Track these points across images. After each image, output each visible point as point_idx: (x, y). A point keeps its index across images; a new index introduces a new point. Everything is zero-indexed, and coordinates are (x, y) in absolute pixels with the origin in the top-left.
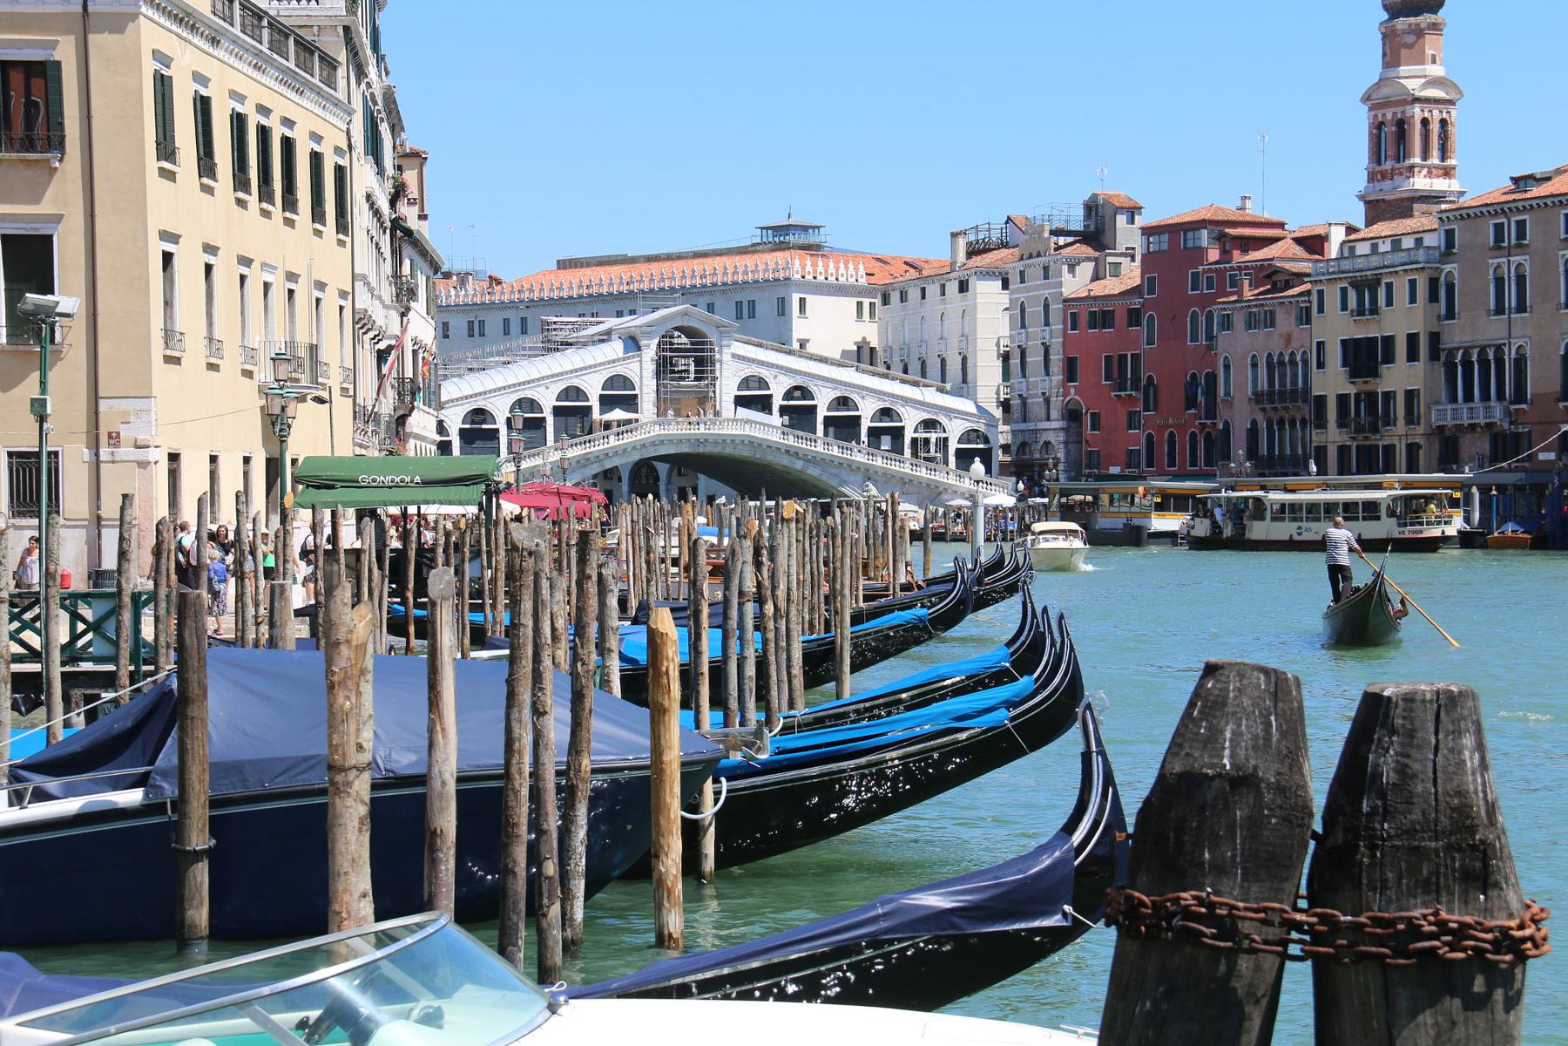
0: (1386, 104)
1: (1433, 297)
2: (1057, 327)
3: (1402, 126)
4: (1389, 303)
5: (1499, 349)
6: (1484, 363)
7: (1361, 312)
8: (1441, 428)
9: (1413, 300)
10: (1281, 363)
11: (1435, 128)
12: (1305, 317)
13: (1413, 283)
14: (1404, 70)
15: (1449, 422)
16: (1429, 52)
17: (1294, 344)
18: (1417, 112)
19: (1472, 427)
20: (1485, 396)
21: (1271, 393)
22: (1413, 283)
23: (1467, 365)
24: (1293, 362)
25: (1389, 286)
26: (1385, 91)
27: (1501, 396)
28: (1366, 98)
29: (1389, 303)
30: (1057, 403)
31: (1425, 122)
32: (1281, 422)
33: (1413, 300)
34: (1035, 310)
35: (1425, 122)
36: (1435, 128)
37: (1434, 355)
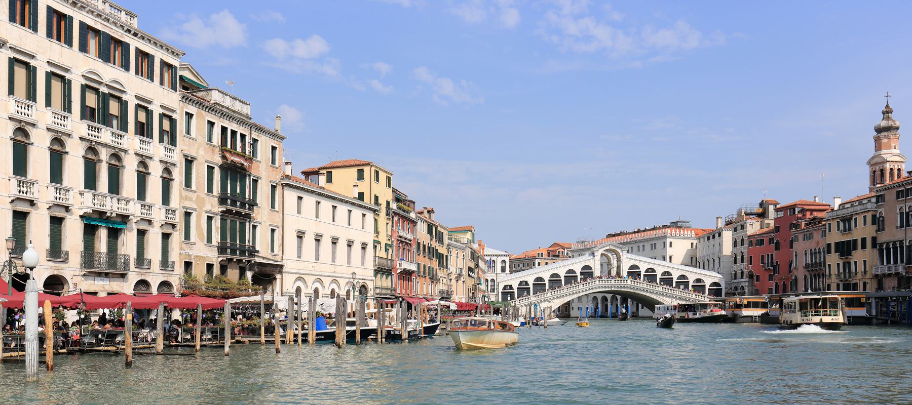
0: (877, 164)
1: (874, 223)
2: (746, 245)
3: (882, 171)
4: (856, 226)
5: (901, 242)
6: (895, 248)
7: (845, 231)
8: (877, 276)
9: (865, 224)
10: (815, 253)
11: (895, 172)
12: (824, 234)
13: (865, 217)
14: (883, 152)
15: (879, 272)
16: (893, 145)
17: (820, 246)
18: (888, 166)
19: (890, 275)
20: (896, 261)
21: (812, 264)
22: (865, 217)
23: (888, 249)
24: (820, 252)
25: (856, 219)
26: (876, 160)
27: (902, 262)
28: (869, 163)
29: (856, 226)
30: (746, 272)
31: (891, 170)
32: (815, 275)
33: (865, 224)
34: (739, 241)
35: (891, 170)
36: (895, 172)
37: (874, 245)
